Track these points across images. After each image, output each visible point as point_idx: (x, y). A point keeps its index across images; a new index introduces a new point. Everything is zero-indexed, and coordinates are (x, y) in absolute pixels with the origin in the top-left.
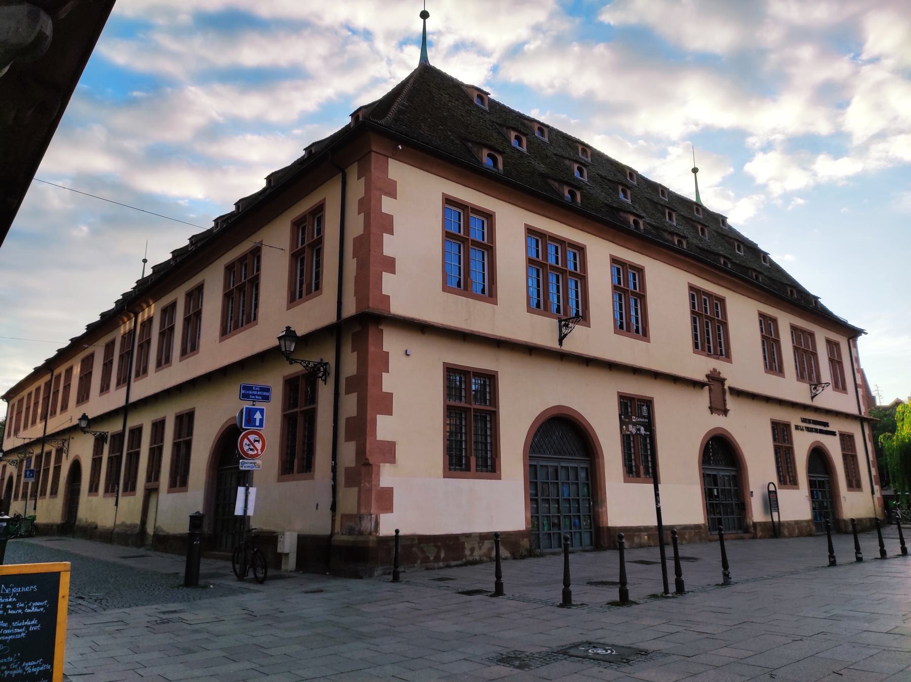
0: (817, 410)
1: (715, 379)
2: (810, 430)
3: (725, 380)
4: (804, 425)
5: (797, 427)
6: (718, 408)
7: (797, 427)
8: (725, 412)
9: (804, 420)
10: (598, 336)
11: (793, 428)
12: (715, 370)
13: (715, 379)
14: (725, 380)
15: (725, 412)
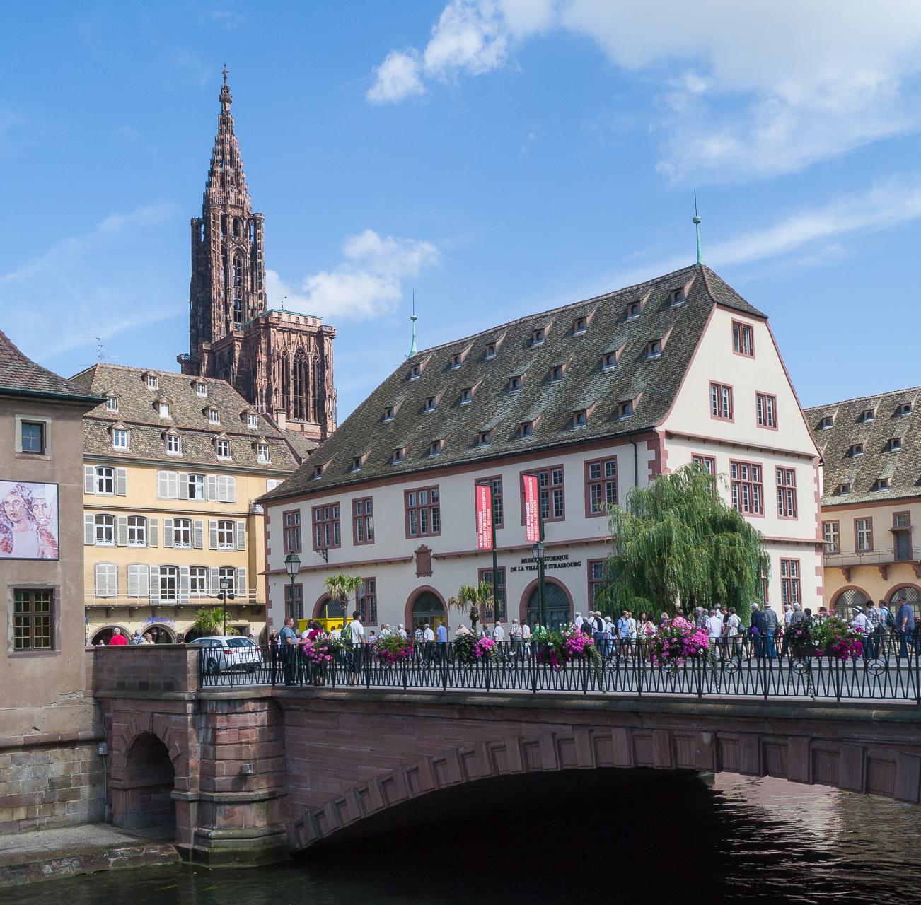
0: (548, 547)
1: (423, 552)
2: (530, 568)
3: (431, 551)
4: (524, 565)
5: (514, 569)
6: (424, 571)
7: (514, 569)
8: (430, 573)
9: (523, 561)
10: (348, 550)
11: (508, 571)
12: (423, 546)
13: (423, 552)
14: (431, 551)
15: (430, 573)
